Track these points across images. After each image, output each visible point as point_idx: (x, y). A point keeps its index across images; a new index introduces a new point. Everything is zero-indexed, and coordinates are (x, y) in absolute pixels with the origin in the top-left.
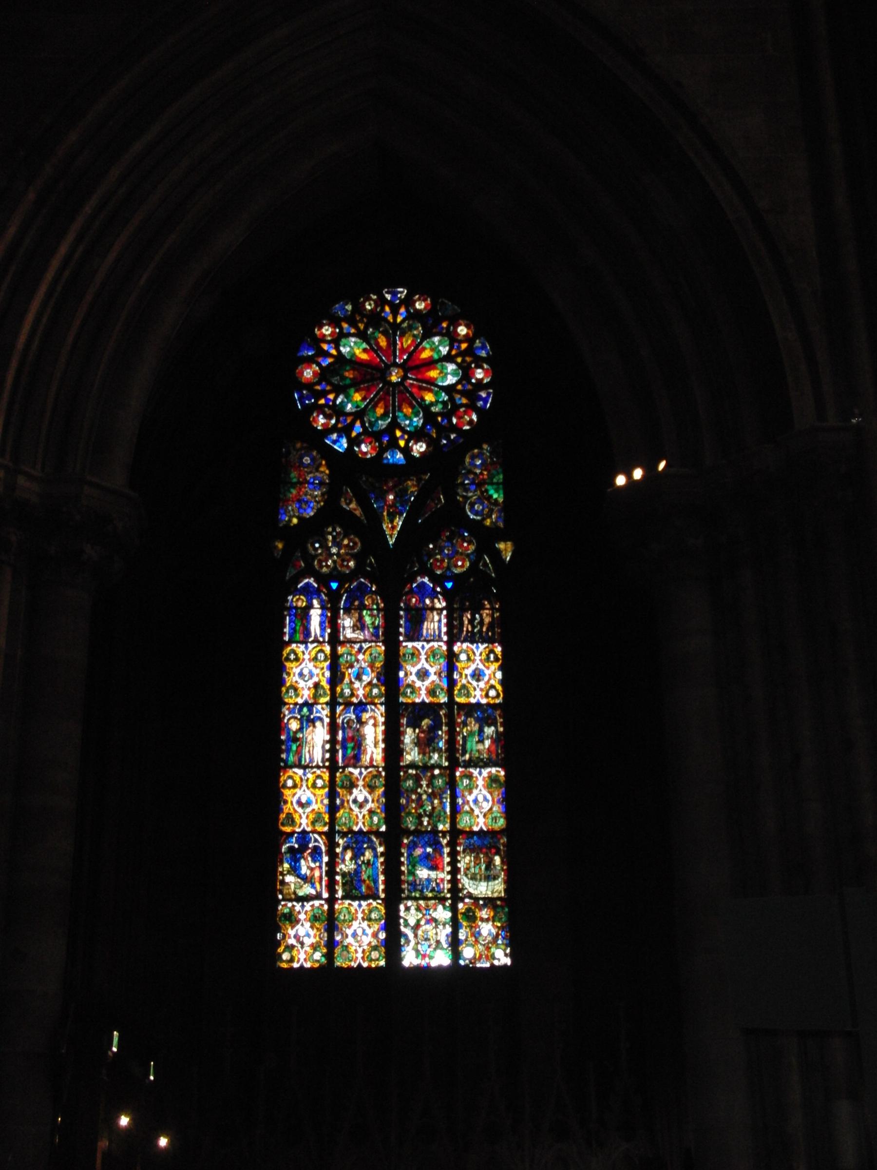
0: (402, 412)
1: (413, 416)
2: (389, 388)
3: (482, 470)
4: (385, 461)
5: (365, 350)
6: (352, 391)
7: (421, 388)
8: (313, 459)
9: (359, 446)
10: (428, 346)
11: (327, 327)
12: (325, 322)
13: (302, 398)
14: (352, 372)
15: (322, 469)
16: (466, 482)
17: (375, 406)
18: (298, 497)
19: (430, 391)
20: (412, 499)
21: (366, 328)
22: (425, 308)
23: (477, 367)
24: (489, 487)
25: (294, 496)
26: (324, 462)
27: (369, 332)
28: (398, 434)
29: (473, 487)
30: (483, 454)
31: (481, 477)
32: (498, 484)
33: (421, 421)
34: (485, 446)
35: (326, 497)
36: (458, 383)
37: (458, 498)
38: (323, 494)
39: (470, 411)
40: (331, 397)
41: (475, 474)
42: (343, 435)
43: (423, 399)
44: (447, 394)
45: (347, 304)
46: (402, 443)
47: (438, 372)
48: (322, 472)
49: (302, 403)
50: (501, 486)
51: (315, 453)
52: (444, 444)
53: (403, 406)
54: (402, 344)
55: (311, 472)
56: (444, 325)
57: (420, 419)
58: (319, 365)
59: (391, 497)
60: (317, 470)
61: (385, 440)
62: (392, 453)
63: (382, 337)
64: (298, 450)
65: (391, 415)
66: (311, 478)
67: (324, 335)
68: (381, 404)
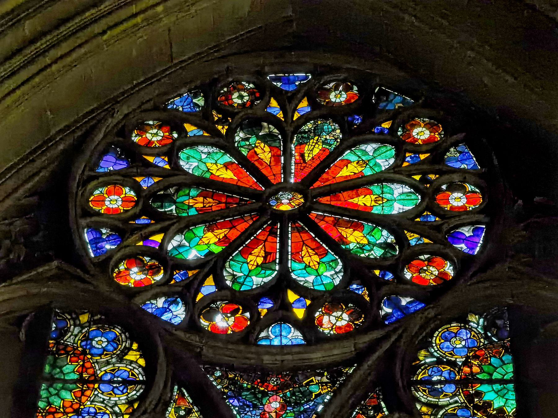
0: (301, 261)
1: (322, 269)
2: (274, 224)
3: (467, 357)
4: (264, 343)
5: (227, 166)
6: (199, 230)
7: (336, 223)
8: (115, 340)
9: (210, 319)
10: (353, 158)
11: (155, 131)
12: (151, 122)
13: (96, 242)
14: (201, 199)
15: (132, 356)
16: (435, 379)
17: (247, 252)
18: (76, 406)
19: (357, 227)
20: (320, 408)
21: (231, 132)
22: (347, 101)
23: (452, 188)
24: (484, 388)
25: (67, 404)
26: (135, 346)
27: (237, 138)
28: (292, 297)
29: (450, 389)
30: (471, 330)
31: (467, 369)
32: (502, 382)
33: (341, 275)
34: (473, 318)
35: (136, 406)
36: (418, 212)
37: (418, 406)
38: (130, 403)
39: (439, 259)
40: (158, 238)
41: (453, 364)
42: (179, 299)
43: (343, 240)
44: (392, 231)
45: (196, 96)
46: (300, 313)
47: (373, 197)
48: (131, 362)
49: (97, 249)
50: (511, 386)
51: (117, 331)
52: (387, 314)
53: (303, 253)
54: (302, 155)
55: (108, 363)
56: (386, 125)
57: (336, 273)
58: (136, 188)
59: (275, 405)
60: (121, 359)
61: (264, 308)
62: (277, 330)
63: (262, 145)
64: (82, 326)
65: (277, 268)
66: (106, 372)
67: (150, 142)
68: (259, 250)
